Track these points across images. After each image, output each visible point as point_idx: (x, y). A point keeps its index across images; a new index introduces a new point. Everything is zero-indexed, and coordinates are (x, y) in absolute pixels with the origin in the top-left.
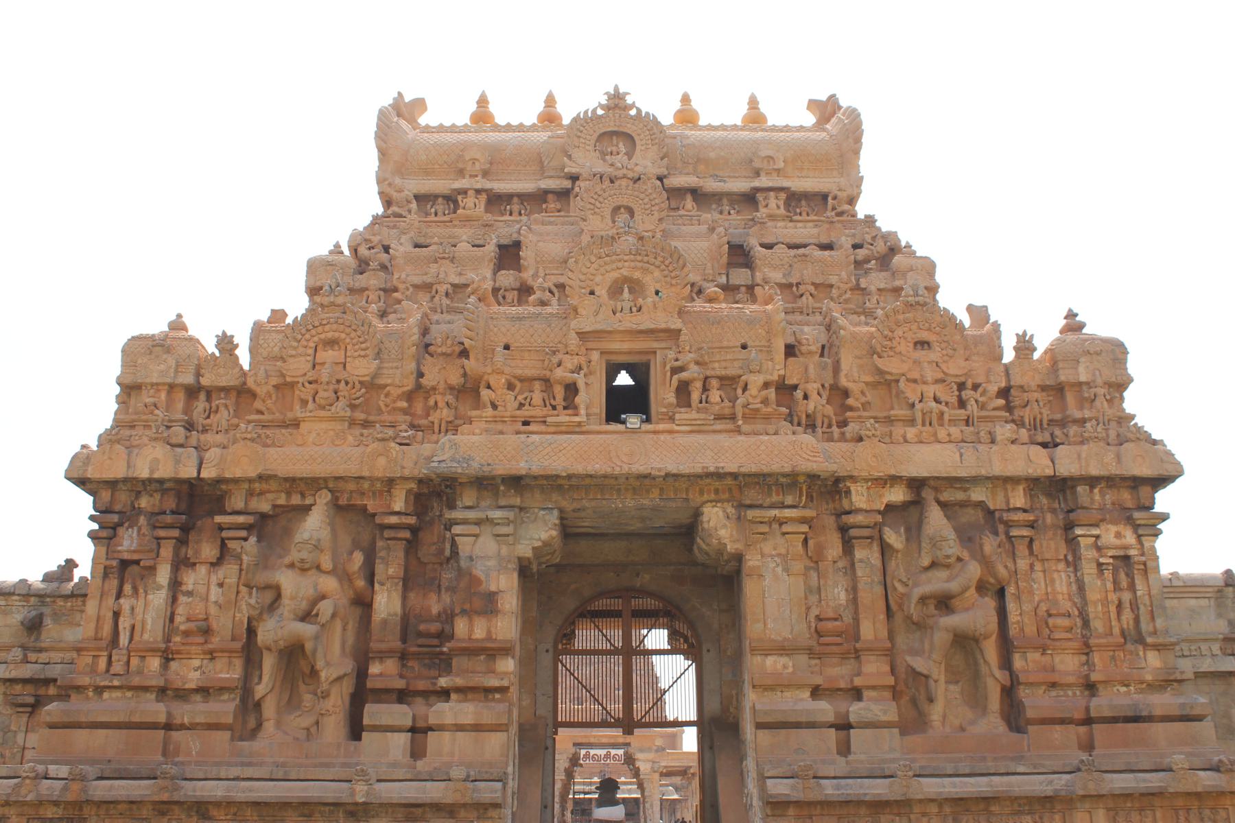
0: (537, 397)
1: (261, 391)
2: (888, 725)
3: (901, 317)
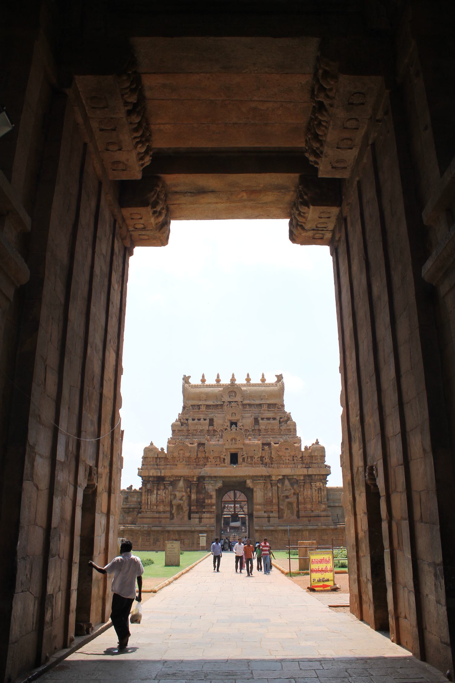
0: (218, 460)
1: (170, 458)
2: (276, 517)
3: (283, 444)
